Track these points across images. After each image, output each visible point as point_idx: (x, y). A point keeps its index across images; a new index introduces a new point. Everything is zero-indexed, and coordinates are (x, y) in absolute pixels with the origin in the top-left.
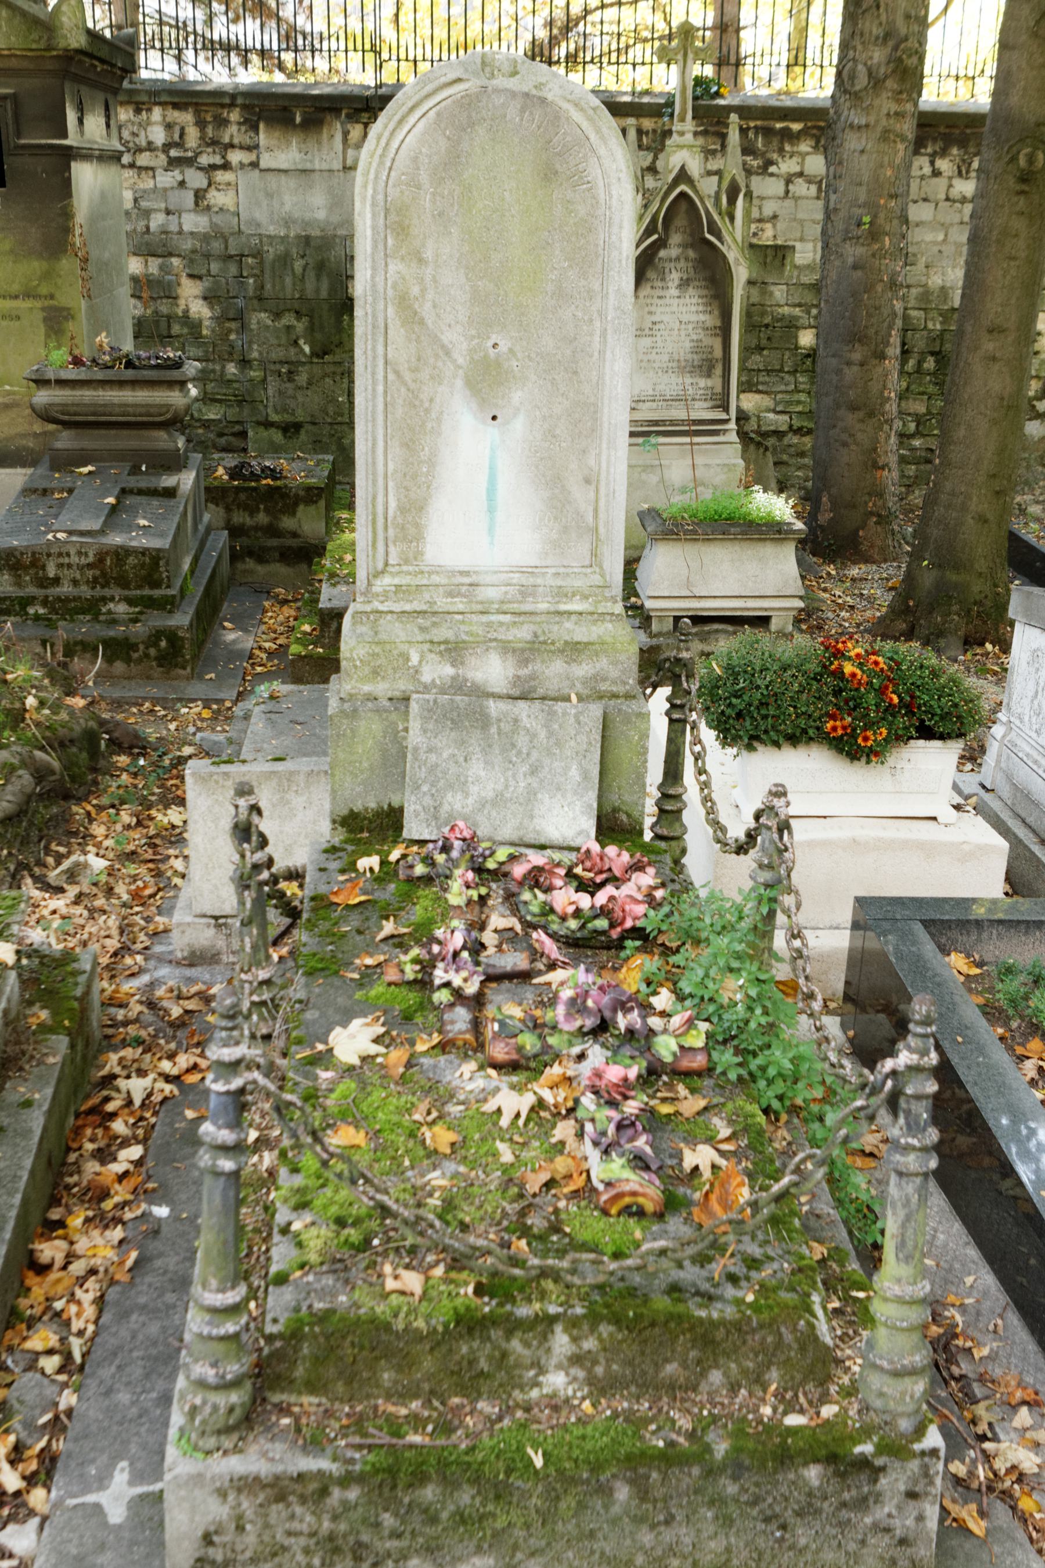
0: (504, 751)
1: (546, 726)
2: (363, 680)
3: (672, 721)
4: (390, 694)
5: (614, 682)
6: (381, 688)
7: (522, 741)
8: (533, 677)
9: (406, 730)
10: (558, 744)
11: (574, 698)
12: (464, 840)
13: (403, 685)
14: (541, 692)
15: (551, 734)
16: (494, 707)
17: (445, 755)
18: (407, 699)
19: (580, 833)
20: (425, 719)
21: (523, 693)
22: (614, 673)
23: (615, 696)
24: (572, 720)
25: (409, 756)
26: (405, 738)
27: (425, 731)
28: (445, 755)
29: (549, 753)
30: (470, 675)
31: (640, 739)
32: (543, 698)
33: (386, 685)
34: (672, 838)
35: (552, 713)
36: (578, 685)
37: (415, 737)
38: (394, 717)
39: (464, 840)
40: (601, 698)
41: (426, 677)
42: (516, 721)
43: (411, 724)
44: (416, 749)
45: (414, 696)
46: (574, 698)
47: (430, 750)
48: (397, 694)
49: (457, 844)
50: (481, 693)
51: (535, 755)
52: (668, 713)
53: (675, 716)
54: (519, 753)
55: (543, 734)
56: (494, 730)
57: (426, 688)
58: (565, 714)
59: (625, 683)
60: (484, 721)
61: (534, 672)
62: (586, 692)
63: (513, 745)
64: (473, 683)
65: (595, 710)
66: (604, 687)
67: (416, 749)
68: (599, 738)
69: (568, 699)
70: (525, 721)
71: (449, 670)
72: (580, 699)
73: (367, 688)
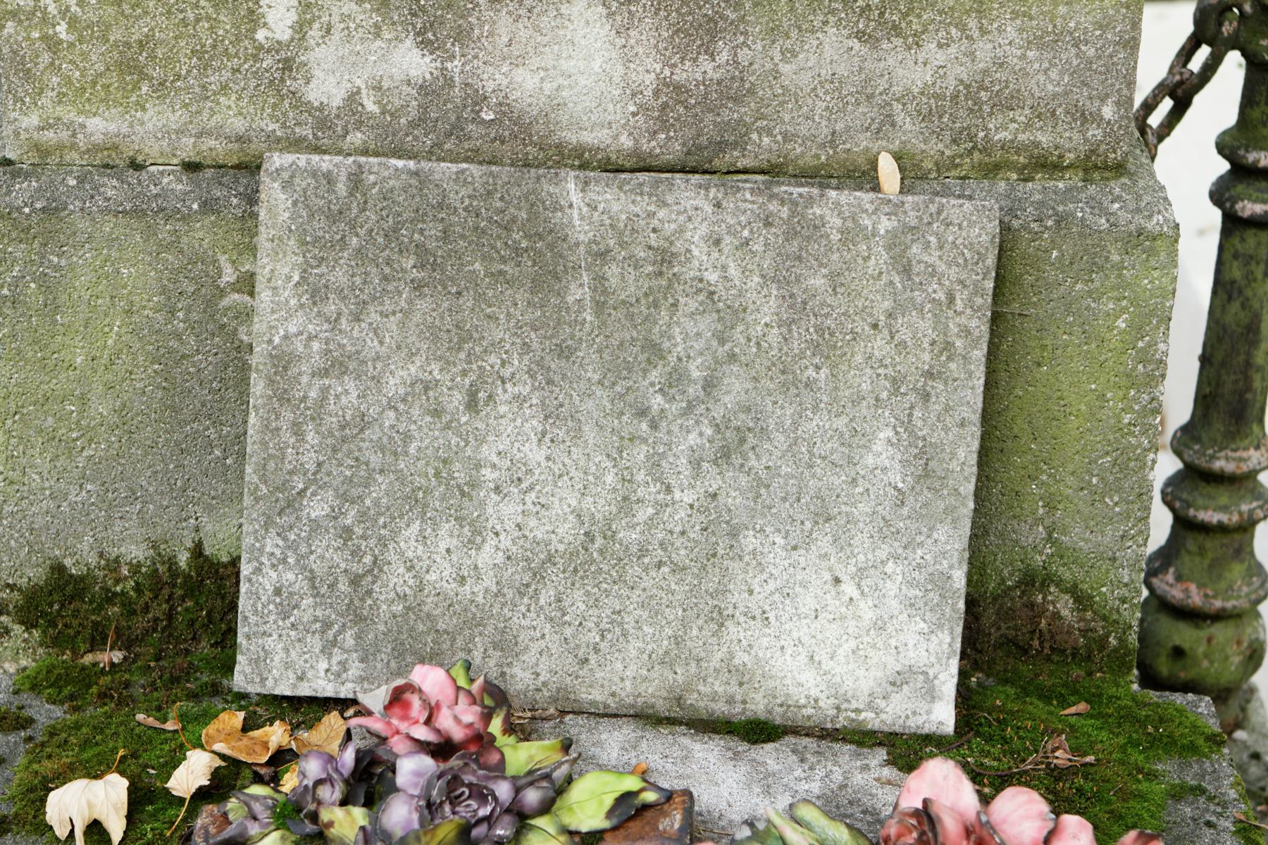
0: (616, 370)
1: (781, 279)
2: (84, 93)
3: (1232, 224)
4: (188, 149)
5: (1044, 114)
6: (155, 126)
7: (688, 334)
8: (734, 89)
9: (247, 284)
10: (825, 346)
11: (888, 171)
12: (442, 749)
13: (235, 116)
14: (763, 146)
15: (797, 308)
16: (582, 205)
17: (393, 385)
18: (250, 168)
19: (897, 682)
20: (318, 249)
21: (698, 149)
22: (1045, 79)
23: (1045, 164)
24: (880, 258)
25: (258, 387)
26: (246, 315)
27: (317, 294)
28: (393, 385)
29: (789, 380)
30: (492, 79)
31: (1137, 329)
32: (773, 171)
33: (176, 118)
34: (1219, 617)
35: (803, 231)
36: (908, 125)
37: (279, 314)
38: (201, 235)
39: (442, 749)
40: (991, 170)
41: (326, 86)
42: (665, 257)
43: (264, 266)
44: (283, 362)
45: (277, 160)
46: (888, 171)
47: (336, 366)
48: (215, 148)
49: (412, 769)
50: (534, 149)
51: (735, 387)
52: (1219, 195)
53: (1249, 208)
54: (676, 379)
55: (766, 309)
56: (579, 291)
57: (324, 132)
58: (850, 235)
59: (1085, 118)
60: (540, 257)
61: (739, 71)
62: (936, 147)
63: (655, 351)
64: (505, 110)
65: (971, 222)
66: (1004, 130)
67: (283, 362)
68: (980, 327)
69: (867, 178)
70: (701, 259)
71: (411, 62)
72: (912, 175)
73: (100, 125)
